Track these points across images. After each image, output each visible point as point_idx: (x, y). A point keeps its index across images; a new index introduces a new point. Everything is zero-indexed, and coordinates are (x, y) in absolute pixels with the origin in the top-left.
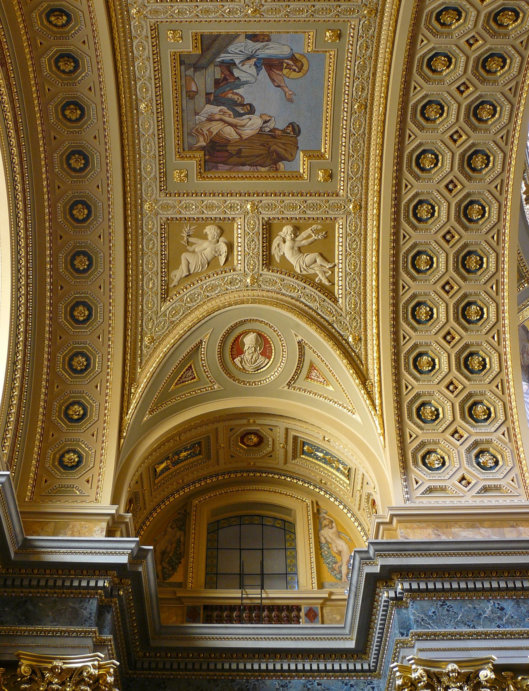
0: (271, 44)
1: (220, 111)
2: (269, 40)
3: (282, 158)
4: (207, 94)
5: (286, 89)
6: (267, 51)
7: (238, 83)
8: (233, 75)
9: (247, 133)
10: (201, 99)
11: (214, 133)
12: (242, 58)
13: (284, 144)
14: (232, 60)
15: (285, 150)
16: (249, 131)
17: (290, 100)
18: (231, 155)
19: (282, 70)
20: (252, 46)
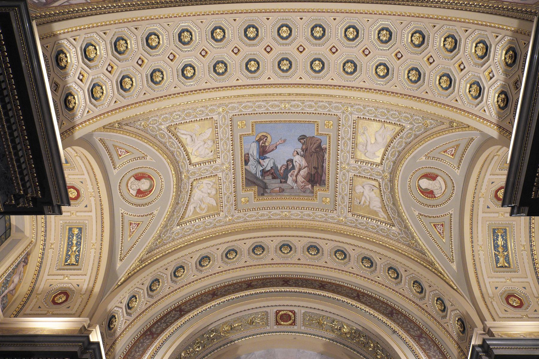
0: (251, 152)
1: (291, 177)
2: (248, 154)
3: (320, 146)
4: (281, 182)
5: (278, 143)
6: (255, 154)
7: (275, 167)
8: (270, 170)
9: (304, 163)
10: (284, 186)
11: (304, 180)
12: (259, 166)
13: (311, 144)
14: (260, 171)
15: (314, 144)
16: (303, 162)
17: (285, 141)
18: (317, 172)
19: (266, 146)
20: (252, 162)
